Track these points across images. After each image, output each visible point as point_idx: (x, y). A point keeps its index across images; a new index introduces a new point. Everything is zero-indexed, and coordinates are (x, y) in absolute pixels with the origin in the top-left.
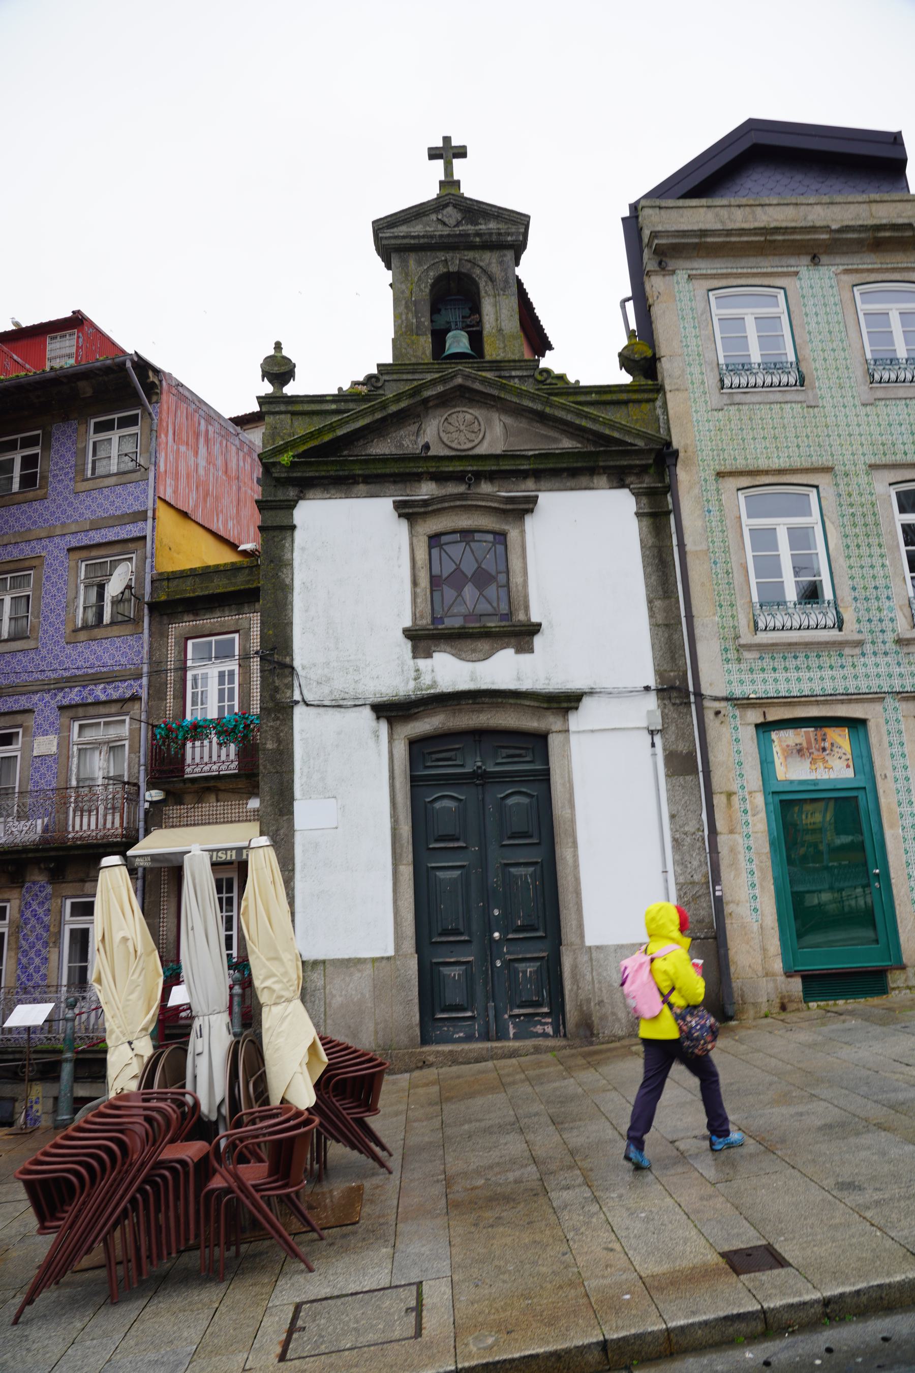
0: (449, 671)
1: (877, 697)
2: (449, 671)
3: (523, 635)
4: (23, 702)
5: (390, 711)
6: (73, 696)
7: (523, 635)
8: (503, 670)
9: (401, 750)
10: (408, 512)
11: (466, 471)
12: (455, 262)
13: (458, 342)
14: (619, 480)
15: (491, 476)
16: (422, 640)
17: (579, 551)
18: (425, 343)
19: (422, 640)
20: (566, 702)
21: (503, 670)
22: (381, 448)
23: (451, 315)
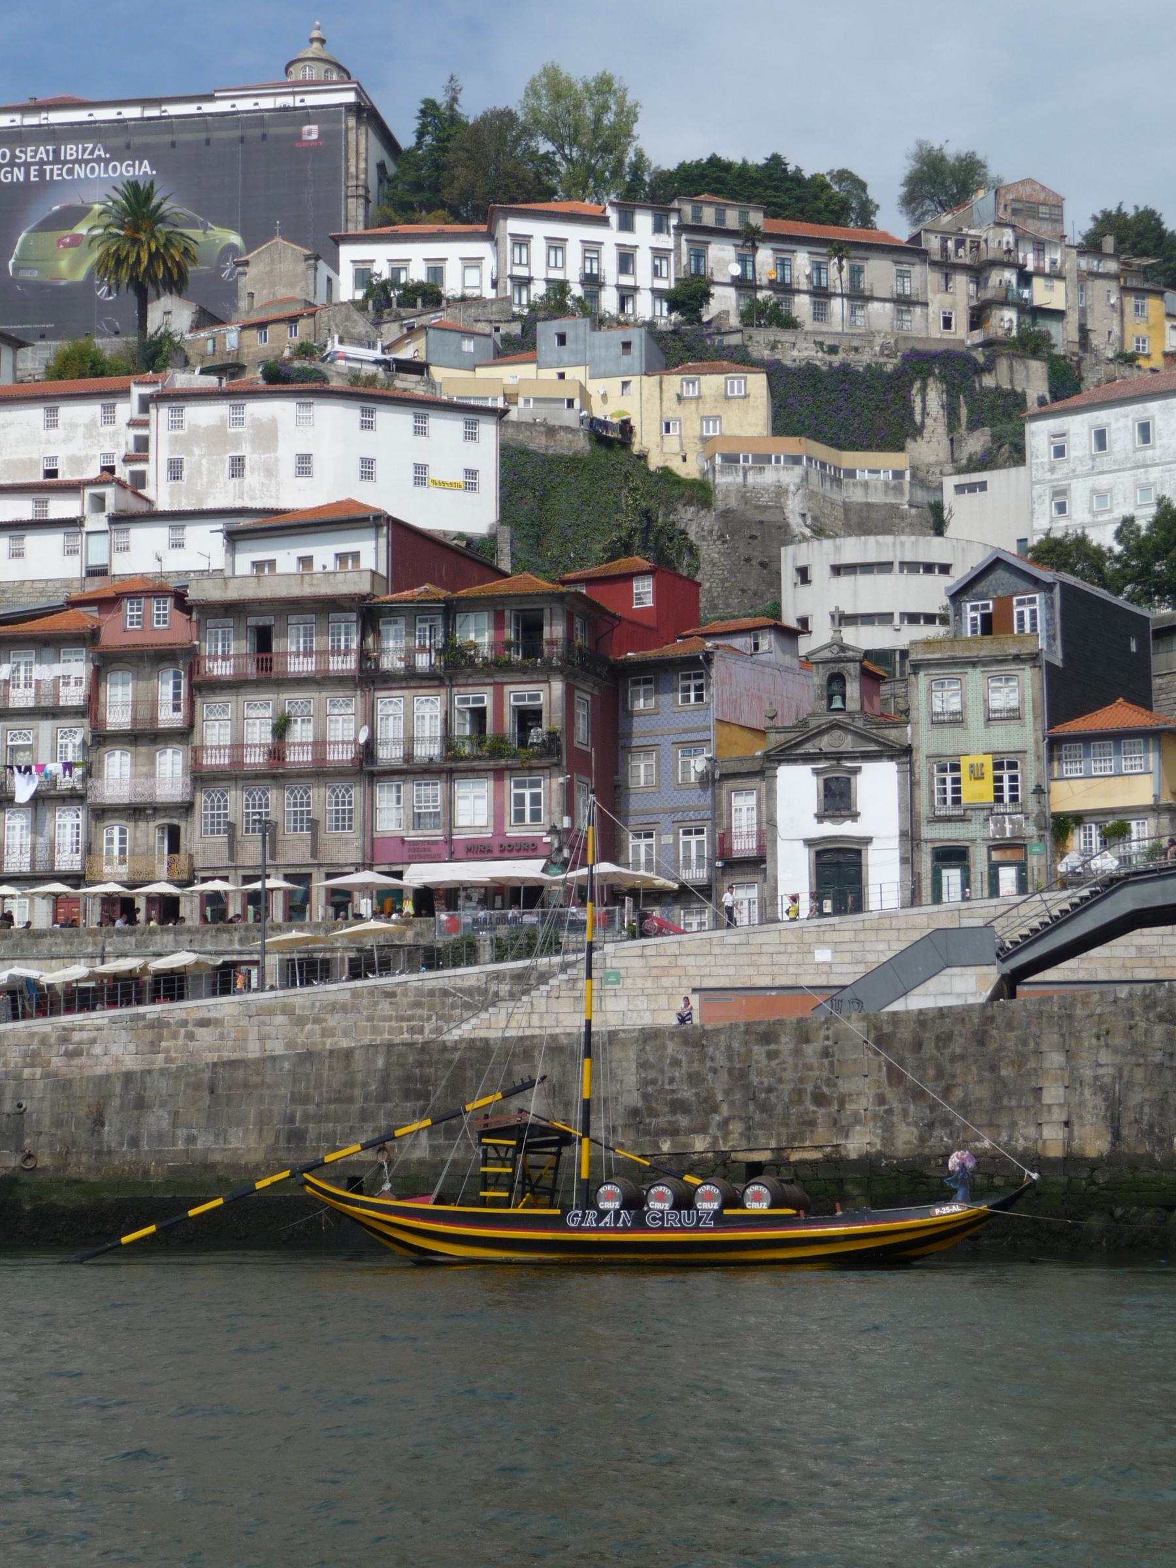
0: (829, 829)
1: (973, 840)
2: (829, 829)
3: (854, 816)
4: (654, 818)
5: (809, 843)
6: (679, 816)
7: (854, 816)
8: (847, 829)
9: (813, 855)
10: (817, 772)
11: (839, 757)
12: (836, 668)
13: (837, 704)
14: (891, 758)
15: (846, 758)
16: (820, 818)
17: (878, 786)
18: (824, 702)
19: (820, 818)
20: (868, 841)
21: (847, 829)
22: (810, 748)
23: (835, 687)
